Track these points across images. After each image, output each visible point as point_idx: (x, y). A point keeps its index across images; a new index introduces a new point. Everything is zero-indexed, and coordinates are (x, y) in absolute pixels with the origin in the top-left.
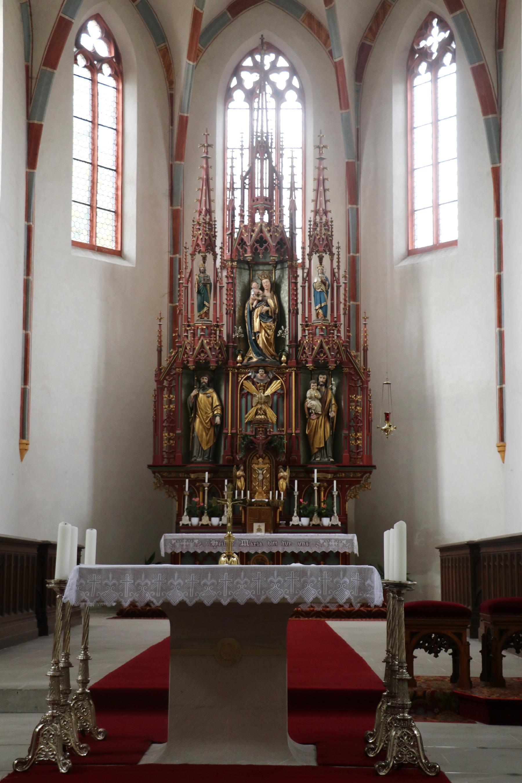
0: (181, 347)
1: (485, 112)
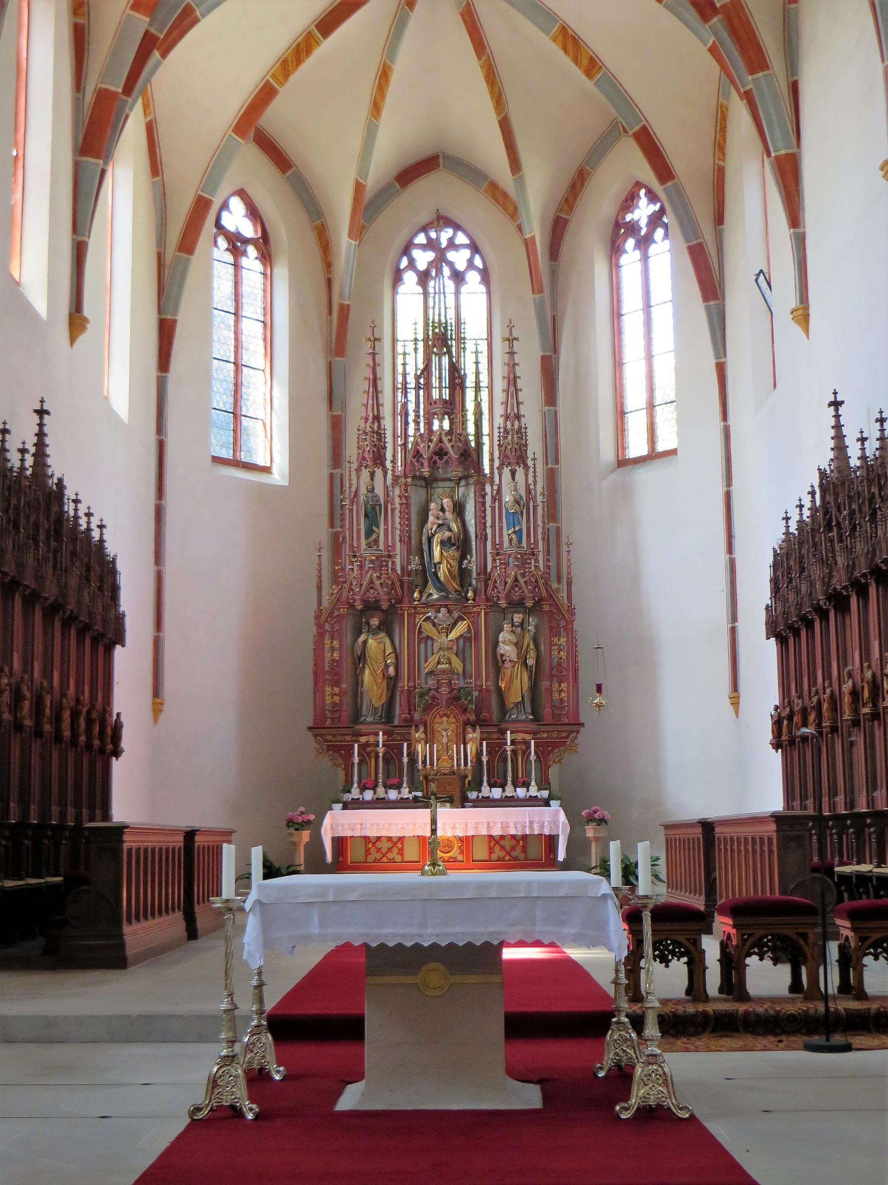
0: (345, 582)
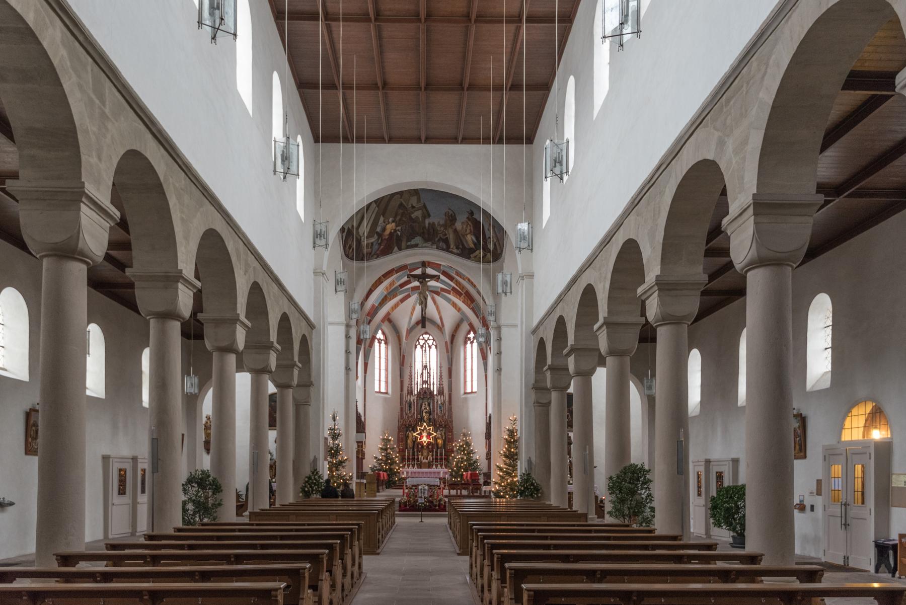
1: (483, 360)
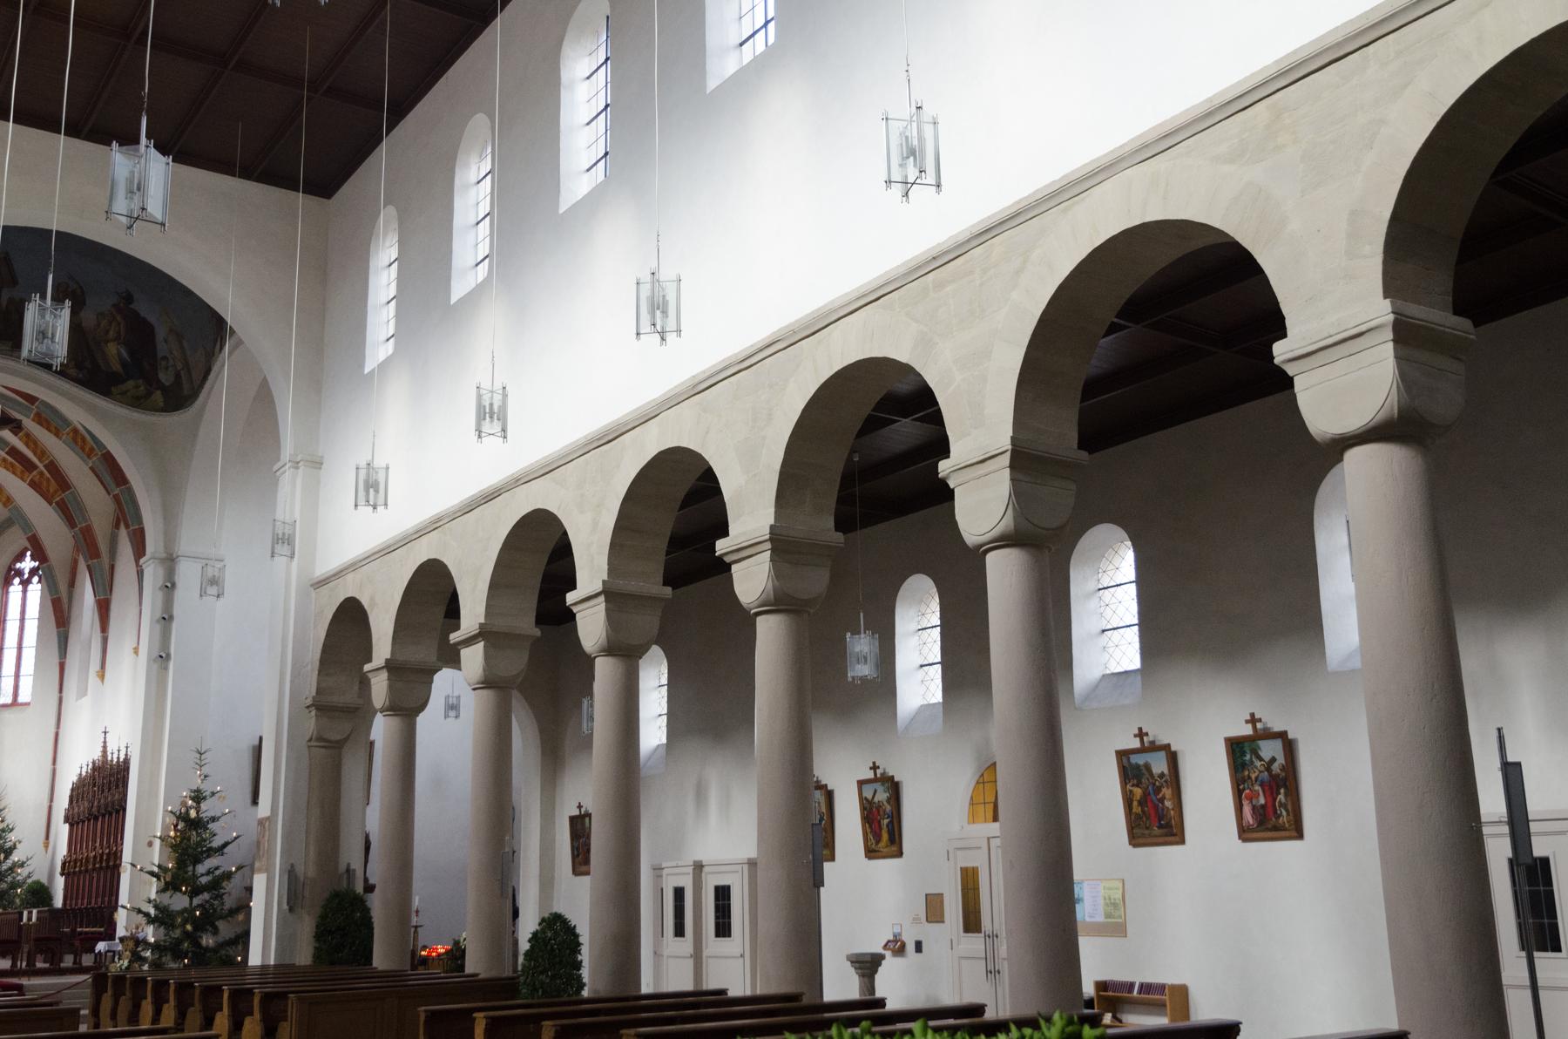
1: (58, 627)
